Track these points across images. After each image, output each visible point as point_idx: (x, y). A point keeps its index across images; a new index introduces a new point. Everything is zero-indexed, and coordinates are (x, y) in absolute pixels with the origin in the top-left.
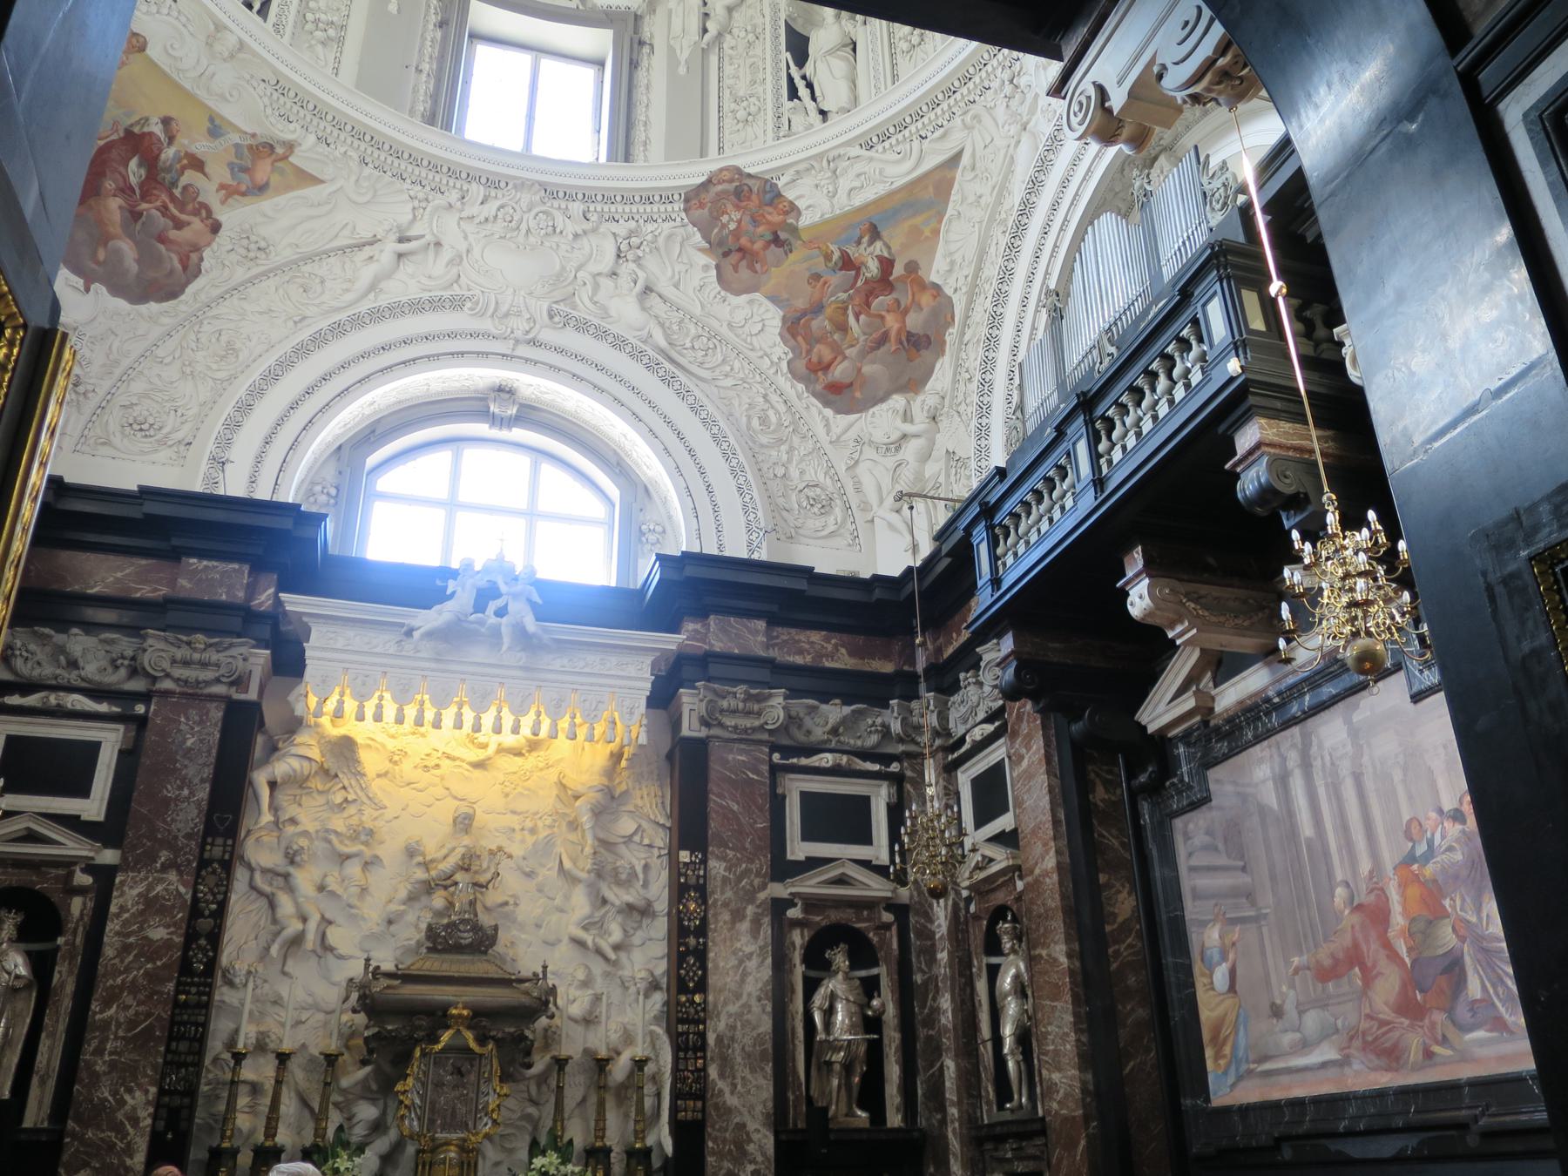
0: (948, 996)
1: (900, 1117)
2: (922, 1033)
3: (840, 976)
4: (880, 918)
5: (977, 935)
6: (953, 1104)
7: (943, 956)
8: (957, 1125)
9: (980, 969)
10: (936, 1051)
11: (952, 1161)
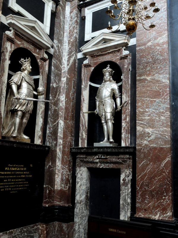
0: (64, 95)
1: (40, 140)
2: (53, 107)
3: (26, 72)
4: (43, 55)
5: (86, 74)
6: (61, 138)
7: (64, 80)
8: (61, 147)
9: (86, 86)
10: (56, 116)
11: (57, 161)
